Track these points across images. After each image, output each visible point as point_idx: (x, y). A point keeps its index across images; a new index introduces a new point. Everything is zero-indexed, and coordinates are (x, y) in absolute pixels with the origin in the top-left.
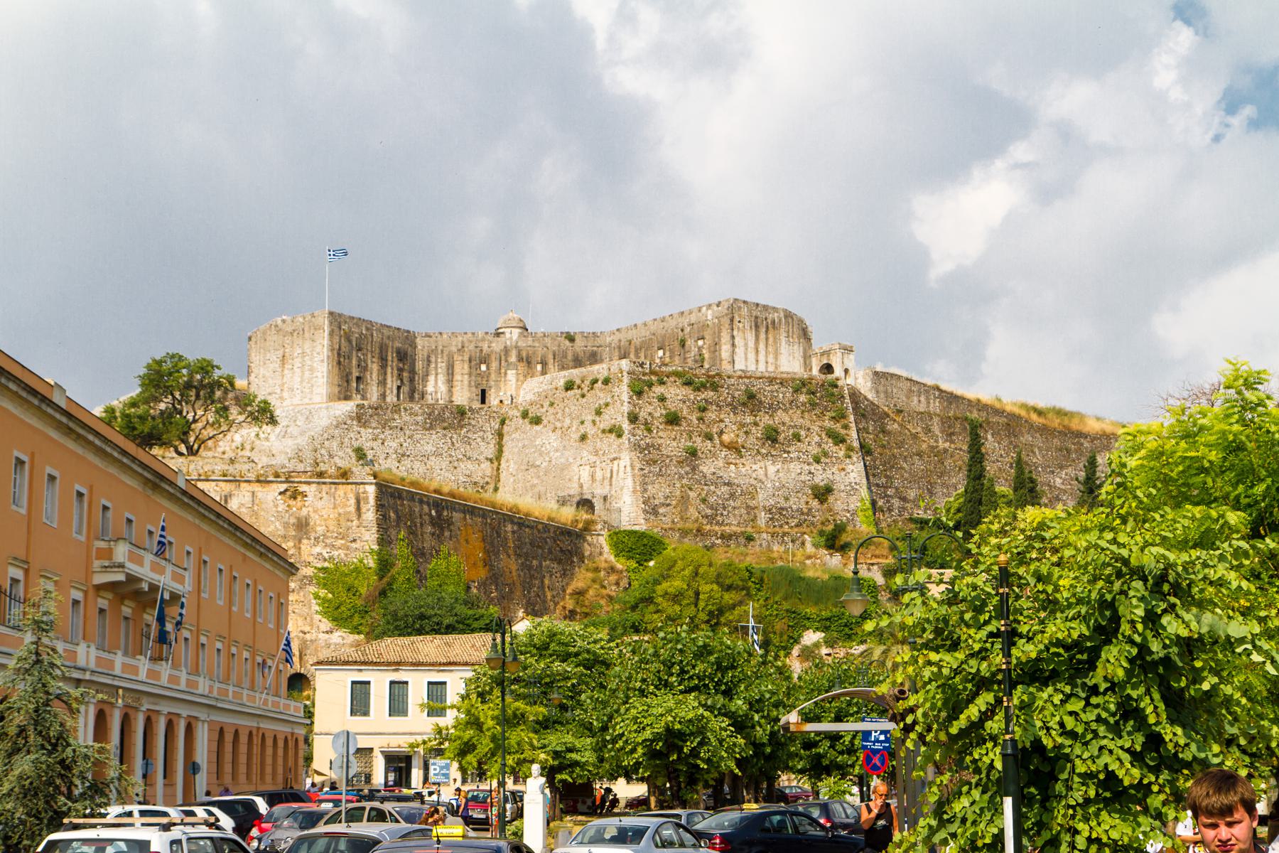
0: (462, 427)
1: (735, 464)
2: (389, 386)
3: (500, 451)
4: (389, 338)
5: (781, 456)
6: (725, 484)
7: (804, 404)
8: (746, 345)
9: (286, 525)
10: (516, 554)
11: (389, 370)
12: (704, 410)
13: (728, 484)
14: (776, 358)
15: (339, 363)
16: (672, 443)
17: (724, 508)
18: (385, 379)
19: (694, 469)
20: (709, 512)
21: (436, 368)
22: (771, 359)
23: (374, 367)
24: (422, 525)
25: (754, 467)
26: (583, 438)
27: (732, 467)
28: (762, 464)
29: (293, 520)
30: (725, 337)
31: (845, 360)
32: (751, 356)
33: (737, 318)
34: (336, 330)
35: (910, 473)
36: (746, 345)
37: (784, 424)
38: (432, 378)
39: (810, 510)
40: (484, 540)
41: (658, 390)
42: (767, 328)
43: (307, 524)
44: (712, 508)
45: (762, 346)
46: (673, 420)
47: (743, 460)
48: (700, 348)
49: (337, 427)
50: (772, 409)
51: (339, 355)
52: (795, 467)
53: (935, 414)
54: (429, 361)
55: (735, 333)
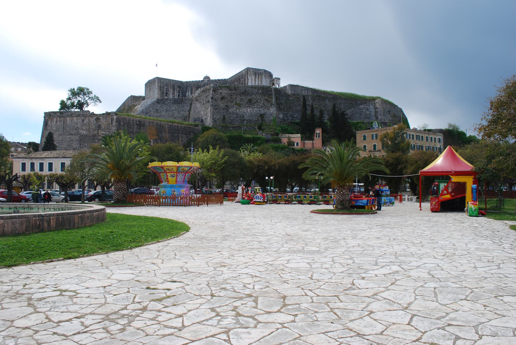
0: (182, 103)
1: (239, 109)
2: (176, 94)
3: (190, 109)
4: (175, 83)
5: (252, 107)
6: (236, 114)
7: (260, 93)
8: (252, 79)
9: (96, 127)
10: (169, 132)
11: (176, 91)
12: (232, 96)
13: (236, 114)
14: (261, 82)
15: (160, 89)
16: (222, 104)
17: (235, 120)
18: (174, 93)
19: (227, 111)
20: (230, 121)
21: (188, 90)
22: (260, 83)
23: (171, 90)
24: (133, 126)
25: (244, 110)
26: (203, 104)
27: (238, 110)
28: (246, 109)
29: (97, 125)
30: (246, 78)
31: (277, 82)
32: (253, 82)
33: (249, 72)
34: (159, 82)
35: (296, 110)
36: (252, 79)
37: (254, 98)
38: (187, 92)
39: (258, 120)
40: (156, 129)
41: (220, 91)
42: (259, 74)
43: (100, 126)
44: (231, 120)
45: (257, 79)
46: (223, 98)
47: (241, 108)
48: (242, 81)
49: (152, 104)
50: (251, 95)
51: (160, 88)
52: (255, 109)
53: (310, 95)
54: (187, 88)
55: (248, 76)
